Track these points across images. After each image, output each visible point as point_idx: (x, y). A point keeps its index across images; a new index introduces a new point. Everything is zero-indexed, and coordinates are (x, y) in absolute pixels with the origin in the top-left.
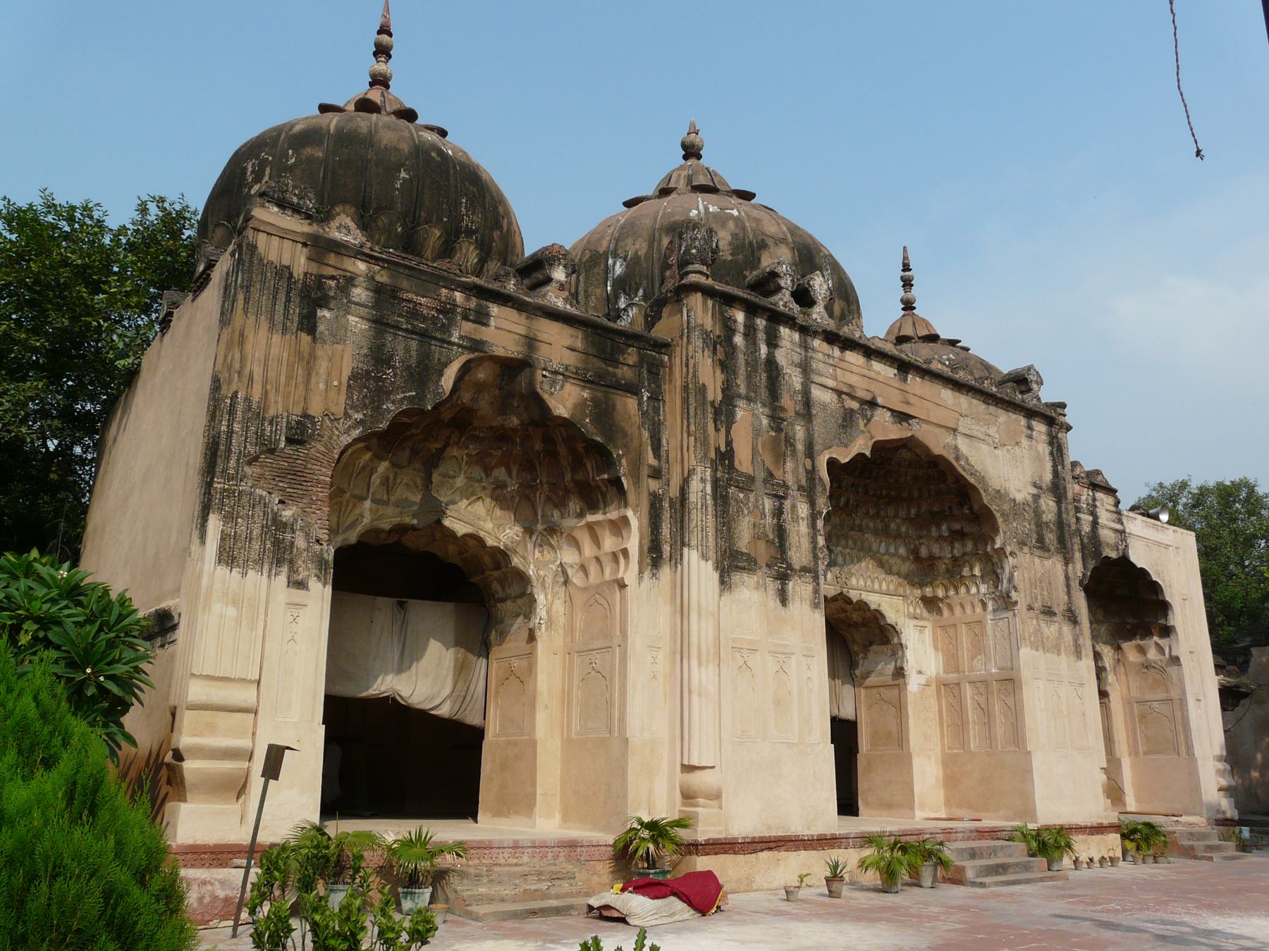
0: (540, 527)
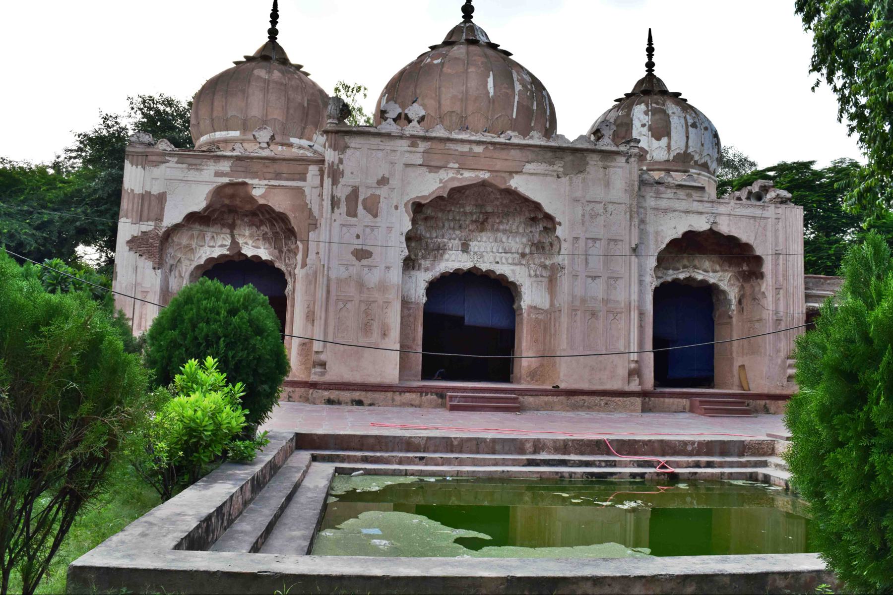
0: (285, 249)
